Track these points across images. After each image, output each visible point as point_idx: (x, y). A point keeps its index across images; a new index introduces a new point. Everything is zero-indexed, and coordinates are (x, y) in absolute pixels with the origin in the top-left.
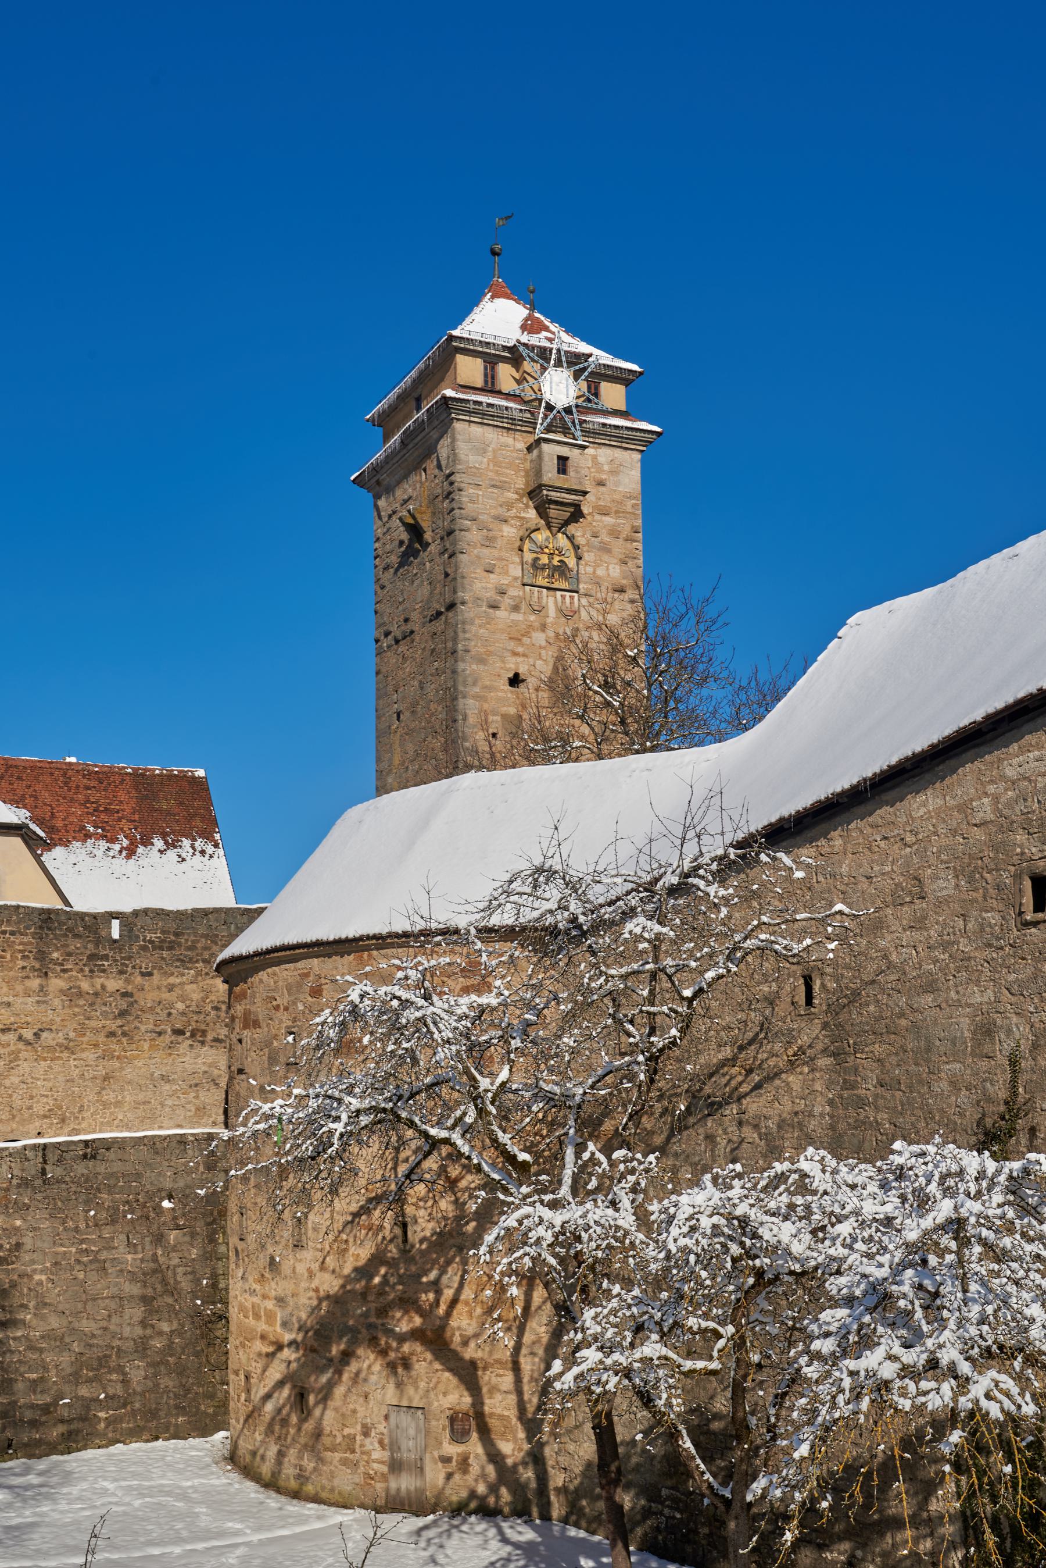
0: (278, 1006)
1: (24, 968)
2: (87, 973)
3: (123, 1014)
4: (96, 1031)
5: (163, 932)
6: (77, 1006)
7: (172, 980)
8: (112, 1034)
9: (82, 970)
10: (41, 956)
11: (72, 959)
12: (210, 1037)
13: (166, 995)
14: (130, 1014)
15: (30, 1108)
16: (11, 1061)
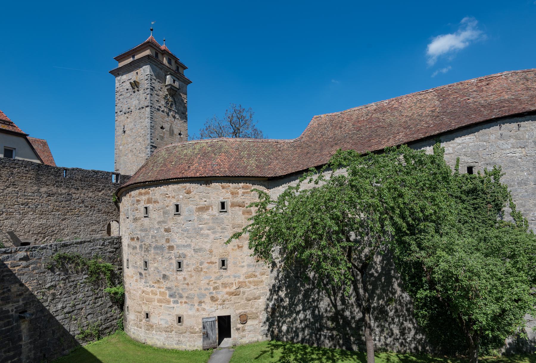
0: (169, 197)
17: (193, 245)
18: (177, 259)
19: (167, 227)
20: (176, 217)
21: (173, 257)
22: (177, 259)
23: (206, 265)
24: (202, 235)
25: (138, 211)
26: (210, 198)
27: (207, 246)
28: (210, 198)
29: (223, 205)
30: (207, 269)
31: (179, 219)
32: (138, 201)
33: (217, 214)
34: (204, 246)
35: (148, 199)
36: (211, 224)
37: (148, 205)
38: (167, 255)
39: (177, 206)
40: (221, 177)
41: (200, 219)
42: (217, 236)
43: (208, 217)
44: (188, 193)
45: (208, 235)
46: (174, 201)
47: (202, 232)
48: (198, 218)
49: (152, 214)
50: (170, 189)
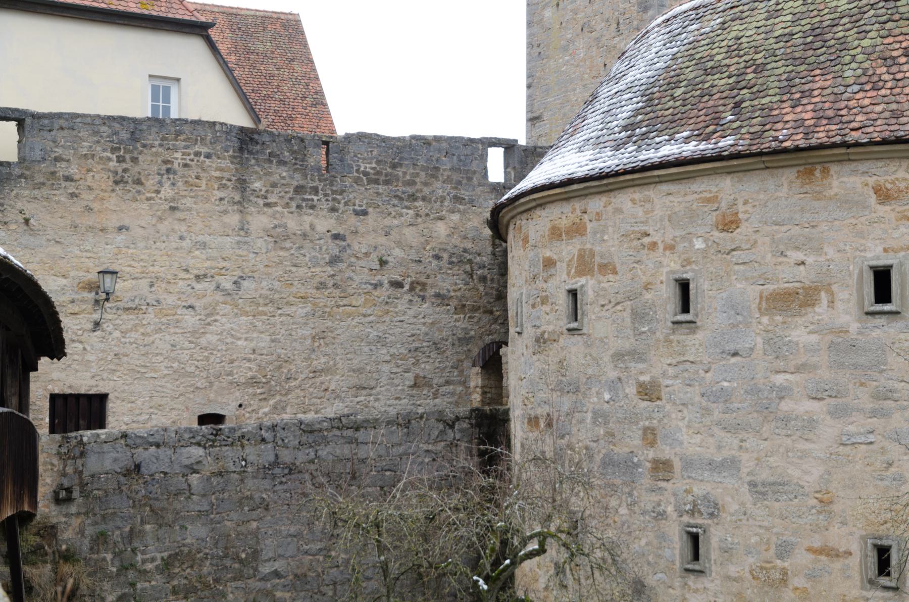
0: (654, 245)
1: (221, 199)
2: (294, 209)
3: (334, 261)
4: (304, 281)
5: (378, 162)
6: (282, 248)
7: (388, 221)
8: (322, 286)
9: (287, 205)
10: (242, 185)
11: (276, 190)
12: (431, 292)
13: (382, 240)
14: (342, 261)
15: (230, 374)
16: (208, 315)
17: (747, 462)
18: (686, 519)
19: (645, 378)
20: (680, 336)
21: (670, 509)
22: (686, 519)
23: (802, 558)
24: (786, 420)
25: (546, 308)
26: (819, 250)
27: (810, 475)
28: (819, 250)
29: (882, 281)
30: (811, 577)
31: (695, 344)
32: (549, 263)
33: (854, 327)
34: (794, 473)
35: (581, 256)
36: (824, 373)
37: (578, 283)
38: (648, 500)
39: (684, 287)
40: (872, 143)
41: (776, 347)
42: (852, 428)
43: (814, 338)
44: (729, 224)
45: (811, 424)
46: (672, 266)
47: (786, 406)
48: (767, 342)
49: (596, 322)
50: (658, 213)
